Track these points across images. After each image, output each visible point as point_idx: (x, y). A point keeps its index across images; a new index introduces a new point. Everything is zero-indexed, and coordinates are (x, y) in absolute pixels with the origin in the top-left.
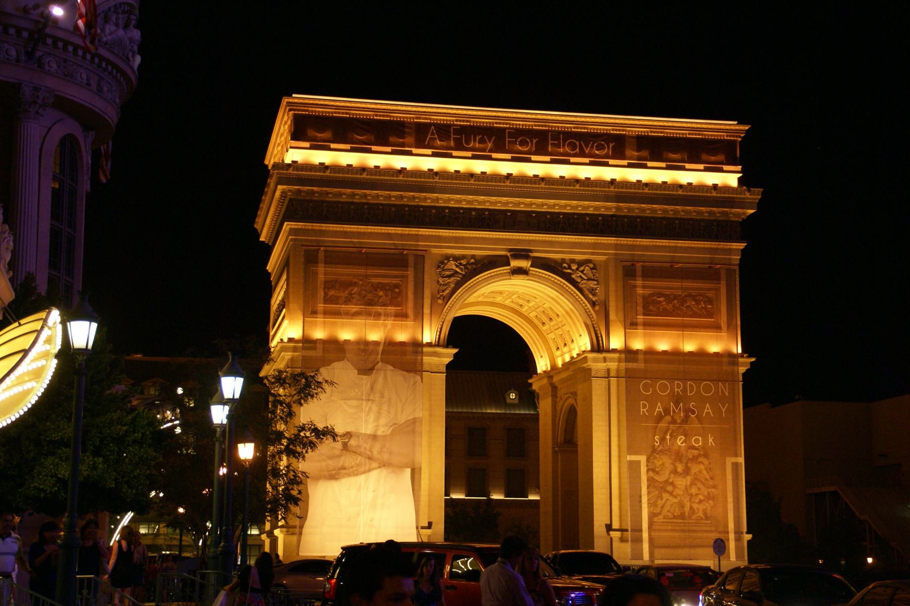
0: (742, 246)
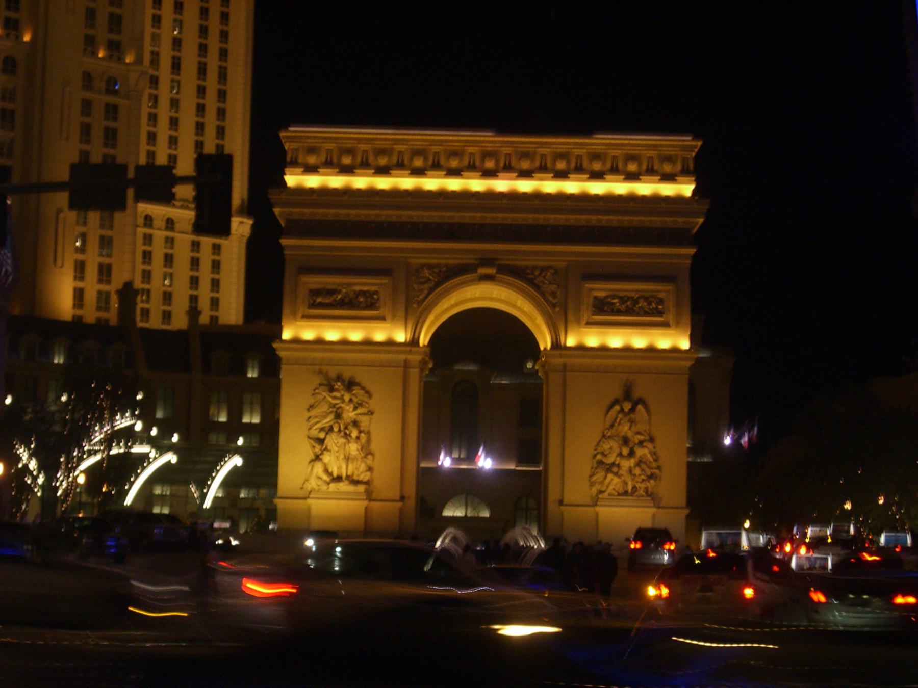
0: (692, 251)
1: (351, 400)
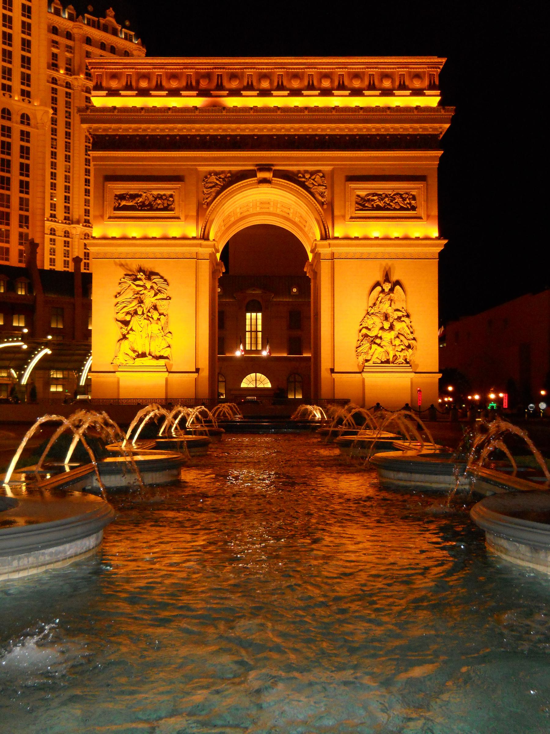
0: (440, 153)
1: (152, 287)
